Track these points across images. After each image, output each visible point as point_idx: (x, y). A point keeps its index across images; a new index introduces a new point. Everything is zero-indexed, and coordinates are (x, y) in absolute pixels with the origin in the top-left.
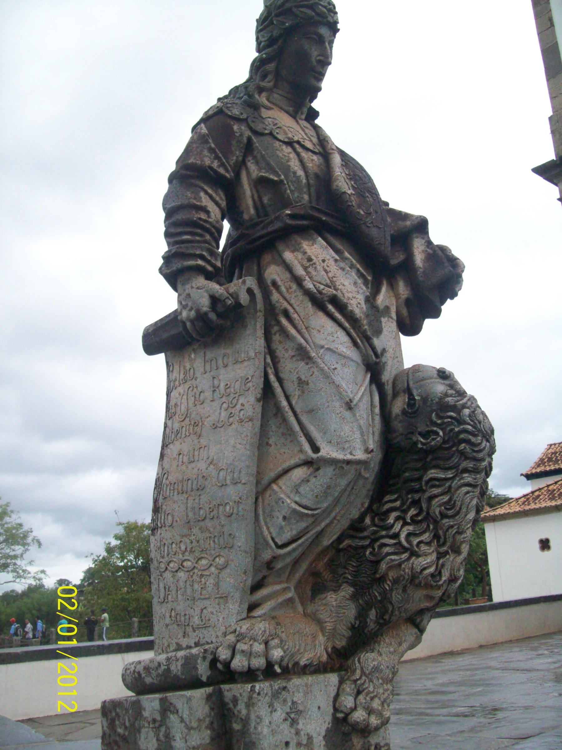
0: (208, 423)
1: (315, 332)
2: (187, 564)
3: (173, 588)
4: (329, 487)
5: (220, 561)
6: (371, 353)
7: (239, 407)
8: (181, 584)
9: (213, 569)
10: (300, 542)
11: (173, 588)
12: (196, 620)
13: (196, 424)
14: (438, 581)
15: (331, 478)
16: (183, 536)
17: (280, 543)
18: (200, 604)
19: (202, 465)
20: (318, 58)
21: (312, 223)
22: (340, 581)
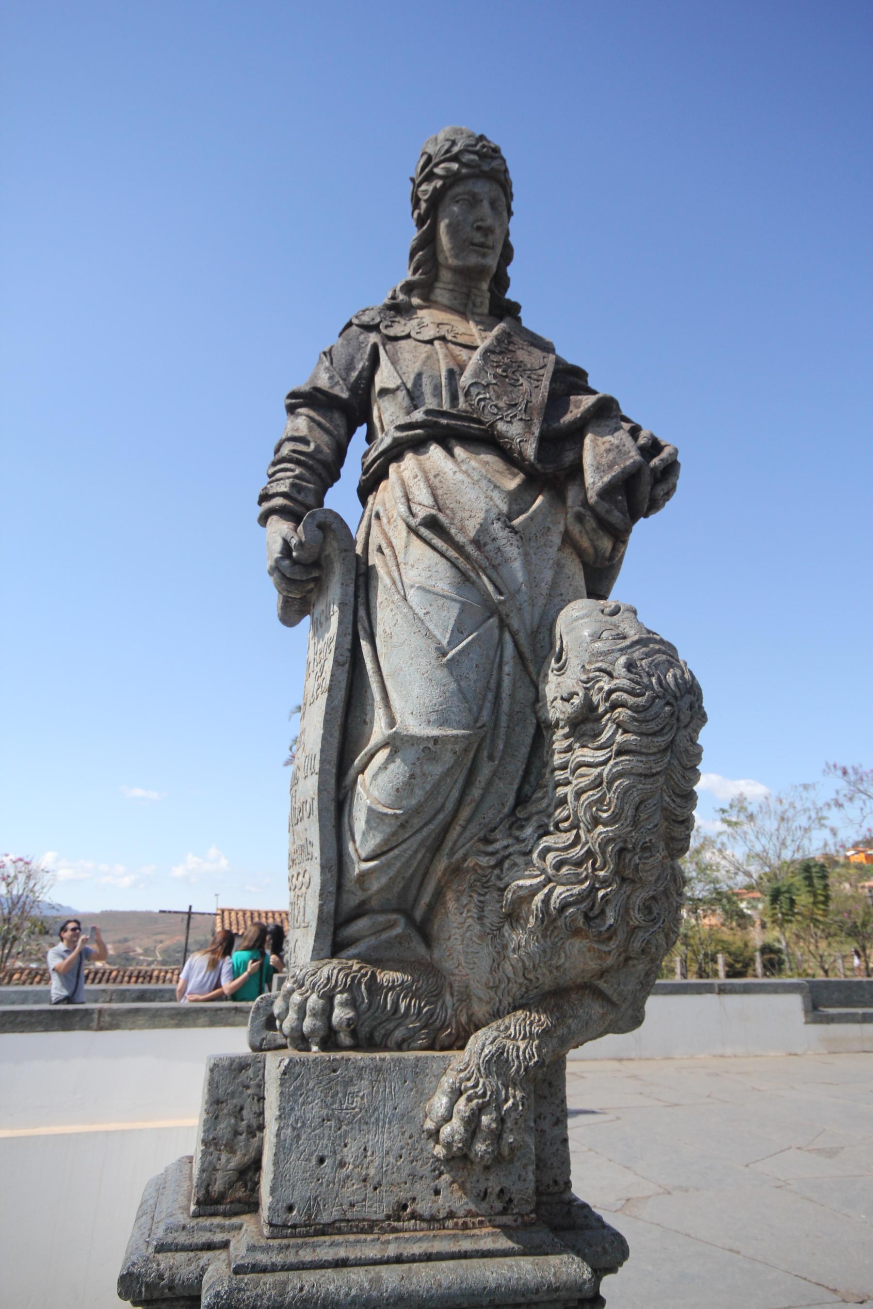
10: (396, 852)
14: (601, 926)
15: (414, 764)
20: (475, 225)
22: (464, 915)
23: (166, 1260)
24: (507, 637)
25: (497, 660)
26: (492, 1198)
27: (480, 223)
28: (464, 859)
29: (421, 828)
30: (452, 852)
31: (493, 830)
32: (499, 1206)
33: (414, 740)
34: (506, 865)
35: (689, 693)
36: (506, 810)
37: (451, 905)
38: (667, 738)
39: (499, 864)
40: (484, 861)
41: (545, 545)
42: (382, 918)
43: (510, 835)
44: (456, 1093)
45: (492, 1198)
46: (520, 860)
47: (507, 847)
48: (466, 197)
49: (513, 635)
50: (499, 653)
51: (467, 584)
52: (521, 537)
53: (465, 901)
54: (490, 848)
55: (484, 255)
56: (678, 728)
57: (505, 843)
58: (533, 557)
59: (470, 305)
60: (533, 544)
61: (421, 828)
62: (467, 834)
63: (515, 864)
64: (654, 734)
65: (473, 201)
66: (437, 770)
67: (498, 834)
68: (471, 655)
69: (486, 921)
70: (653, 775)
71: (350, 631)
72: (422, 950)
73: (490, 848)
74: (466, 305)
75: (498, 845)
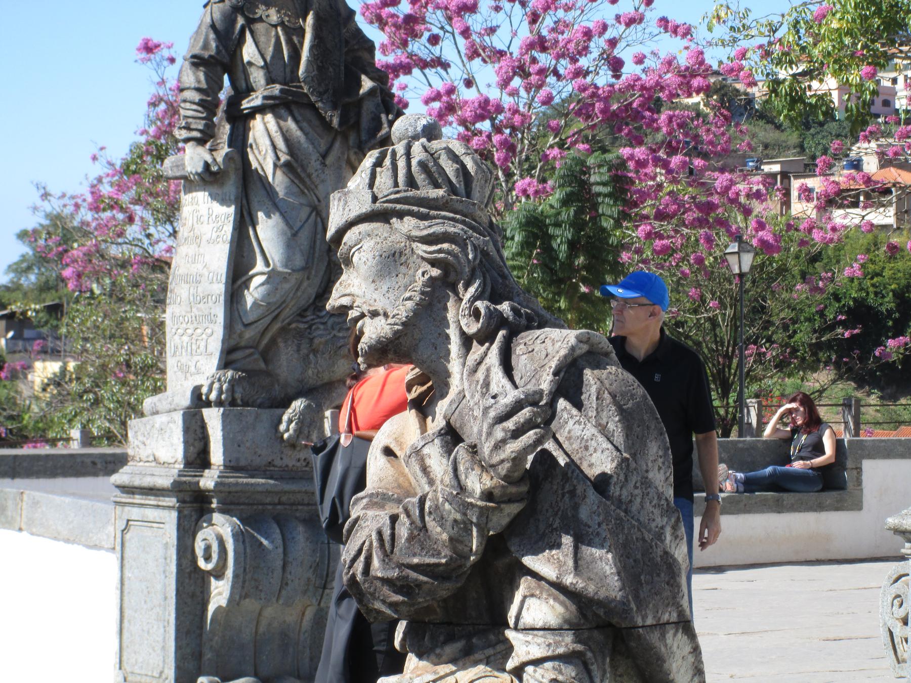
0: (205, 238)
2: (190, 332)
3: (180, 347)
5: (209, 331)
6: (315, 198)
7: (223, 232)
8: (185, 344)
9: (204, 336)
11: (180, 347)
12: (192, 369)
13: (197, 238)
16: (187, 312)
17: (246, 323)
18: (196, 358)
19: (200, 266)
23: (184, 479)
24: (319, 219)
26: (302, 461)
28: (289, 324)
29: (273, 311)
30: (283, 321)
31: (306, 310)
32: (304, 464)
33: (280, 273)
34: (314, 327)
36: (311, 301)
37: (281, 345)
39: (310, 327)
40: (302, 326)
42: (248, 351)
43: (314, 314)
44: (290, 421)
45: (302, 461)
46: (322, 327)
47: (313, 320)
53: (290, 342)
54: (305, 320)
57: (312, 317)
61: (273, 311)
63: (318, 328)
66: (287, 286)
67: (308, 313)
69: (301, 353)
72: (262, 365)
73: (305, 320)
75: (309, 318)
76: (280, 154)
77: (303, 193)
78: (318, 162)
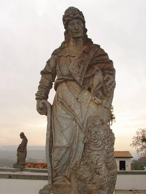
1: (57, 111)
4: (59, 153)
21: (63, 80)
25: (75, 129)
27: (75, 28)
35: (108, 138)
38: (102, 147)
41: (86, 103)
48: (72, 24)
49: (78, 124)
50: (75, 128)
51: (68, 114)
52: (80, 103)
55: (78, 34)
56: (105, 145)
58: (83, 106)
59: (77, 44)
60: (83, 103)
62: (74, 162)
64: (99, 147)
65: (74, 24)
68: (68, 130)
70: (100, 155)
71: (50, 123)
74: (77, 44)
76: (59, 99)
77: (68, 113)
78: (75, 101)
